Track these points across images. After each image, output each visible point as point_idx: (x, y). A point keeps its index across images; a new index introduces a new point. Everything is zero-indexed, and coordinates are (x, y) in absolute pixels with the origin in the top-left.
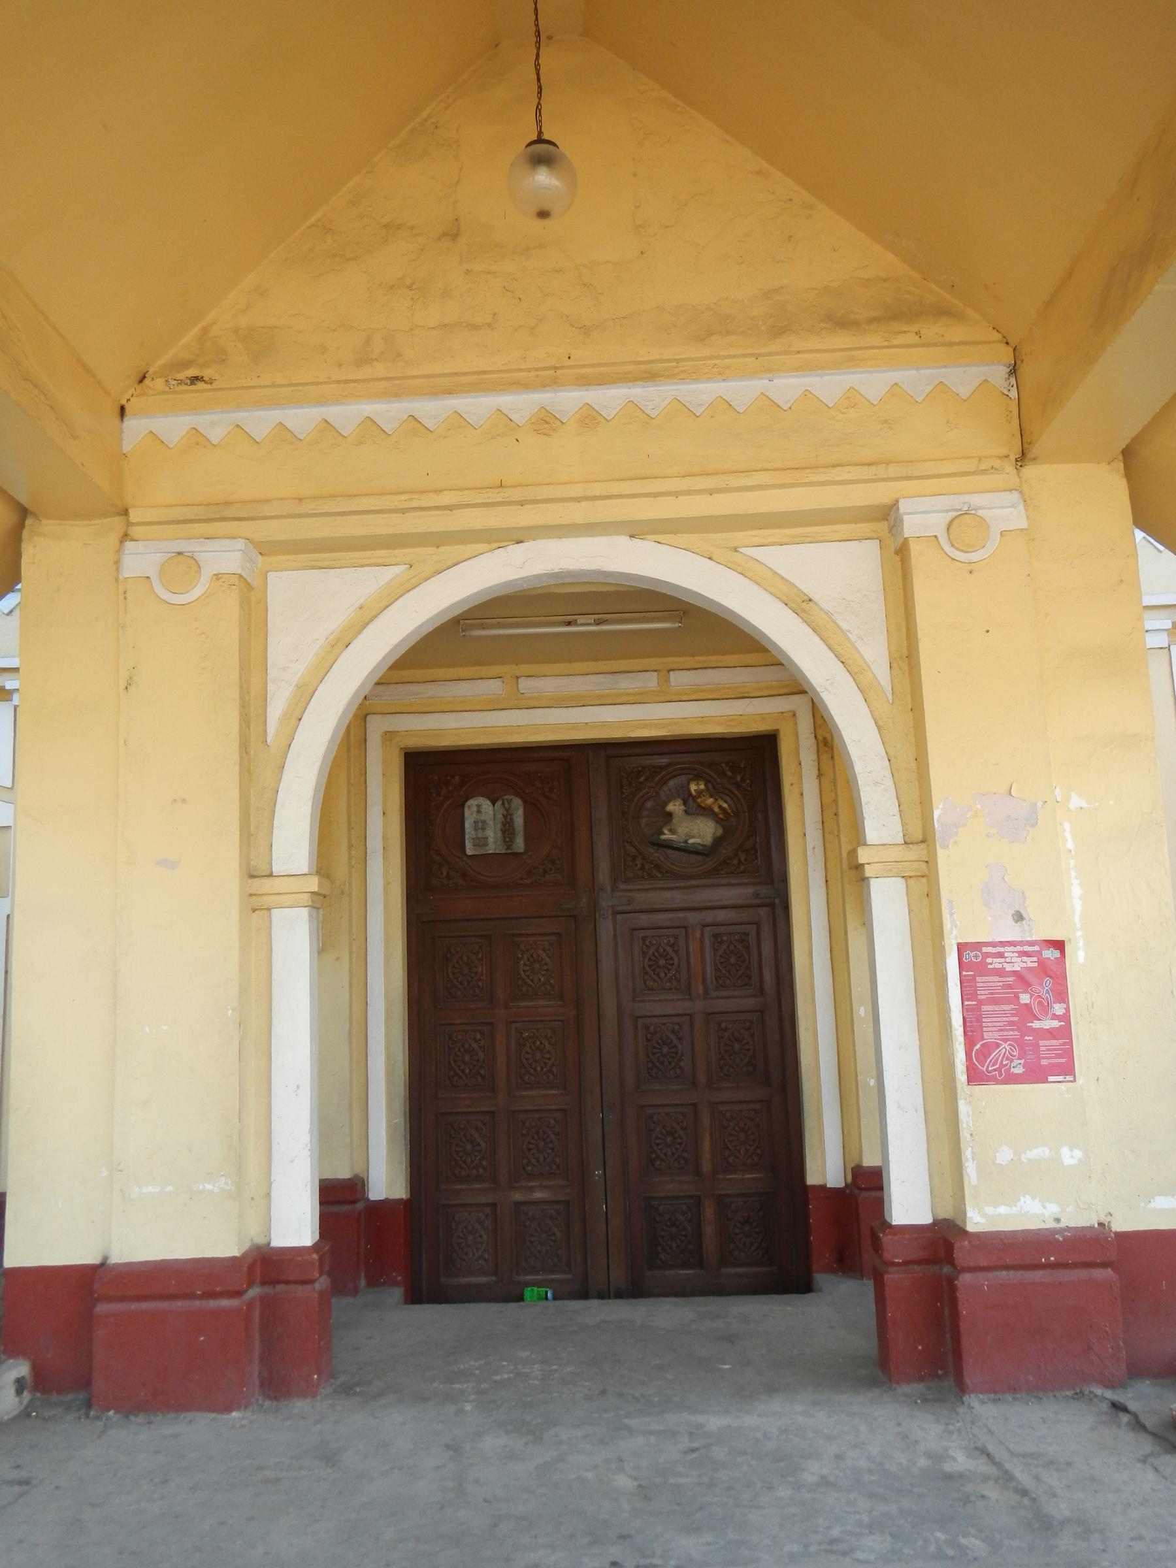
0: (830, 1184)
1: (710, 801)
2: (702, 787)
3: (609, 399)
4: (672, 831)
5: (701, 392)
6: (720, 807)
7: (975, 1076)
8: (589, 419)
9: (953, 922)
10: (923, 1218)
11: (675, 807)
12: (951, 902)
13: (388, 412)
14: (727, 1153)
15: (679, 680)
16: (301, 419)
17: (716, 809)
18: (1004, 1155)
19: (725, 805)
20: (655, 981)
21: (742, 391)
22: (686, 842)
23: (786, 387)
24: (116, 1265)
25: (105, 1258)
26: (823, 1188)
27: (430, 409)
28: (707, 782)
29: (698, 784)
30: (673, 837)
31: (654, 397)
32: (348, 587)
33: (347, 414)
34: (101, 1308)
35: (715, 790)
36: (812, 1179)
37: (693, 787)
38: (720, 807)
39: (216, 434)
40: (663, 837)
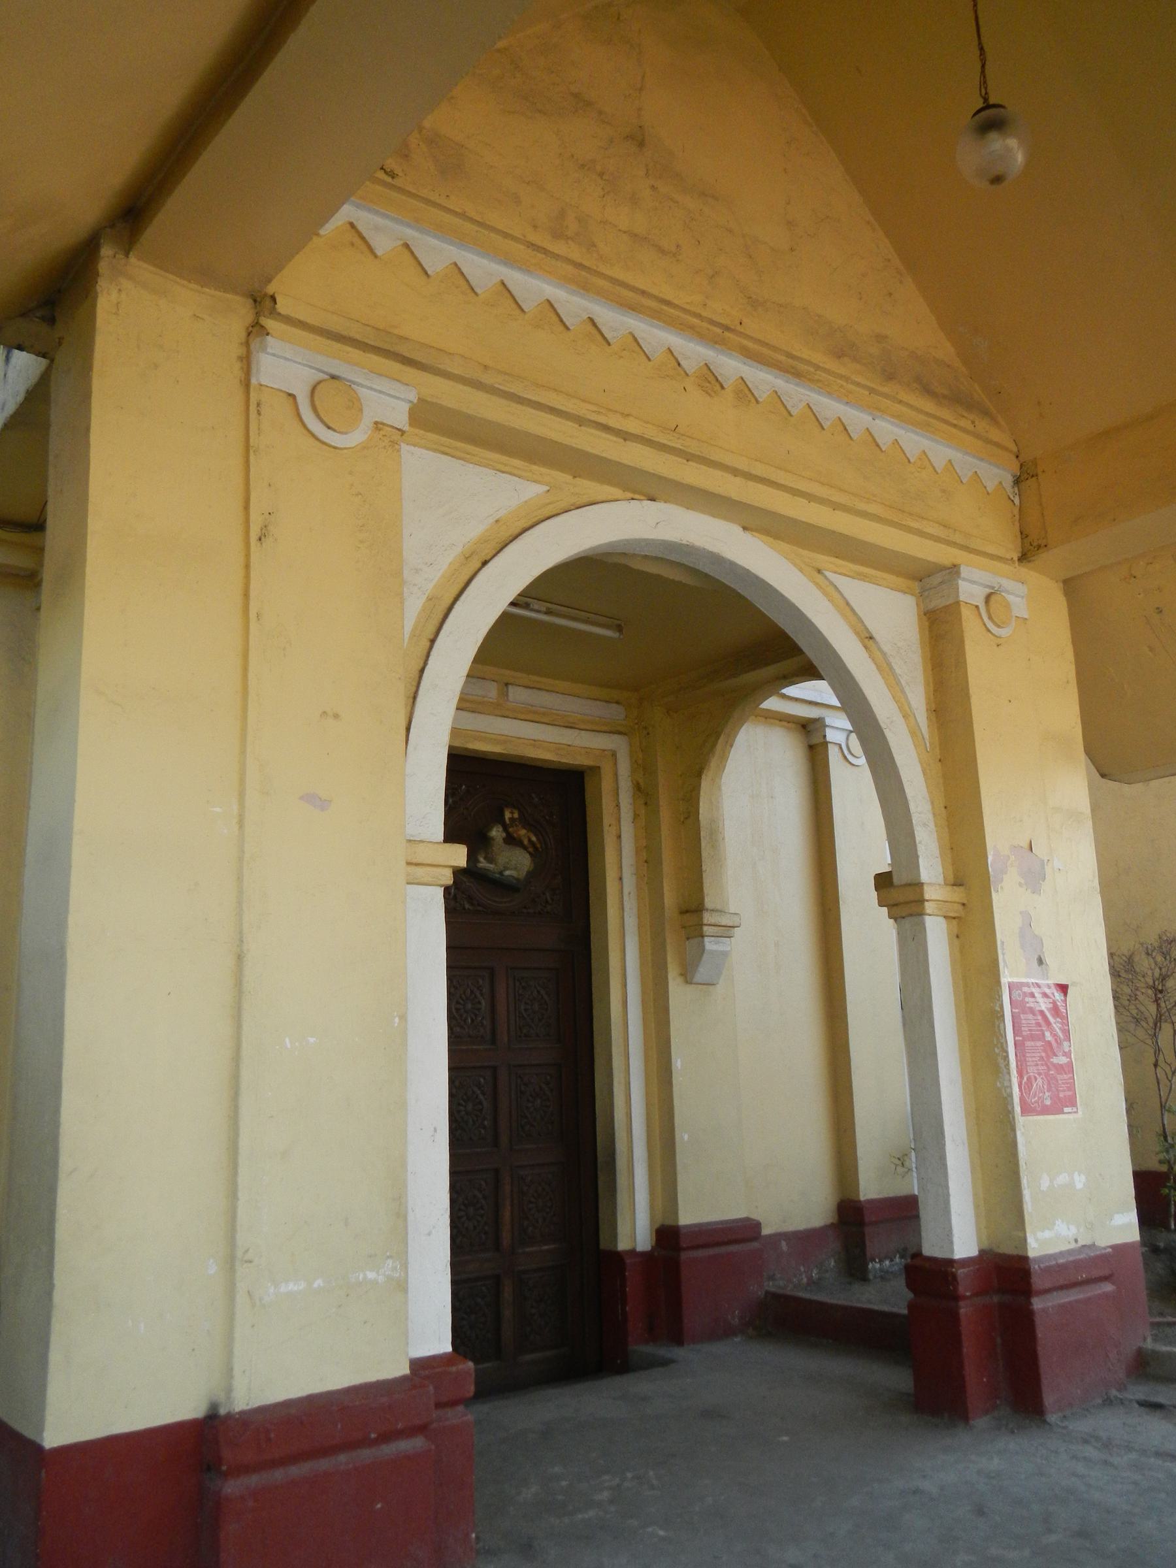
0: (639, 1249)
1: (523, 832)
2: (516, 815)
3: (763, 379)
4: (490, 860)
5: (830, 407)
6: (530, 840)
7: (1026, 1110)
8: (745, 393)
9: (1004, 961)
10: (973, 1252)
11: (496, 833)
12: (1003, 943)
13: (574, 305)
14: (526, 1223)
15: (518, 695)
16: (483, 269)
17: (526, 842)
18: (1045, 1184)
19: (534, 839)
20: (462, 1027)
21: (857, 419)
22: (501, 873)
23: (886, 430)
24: (242, 1413)
25: (213, 1409)
26: (633, 1252)
27: (613, 320)
28: (520, 813)
29: (512, 813)
30: (491, 866)
31: (797, 394)
32: (489, 492)
33: (534, 288)
34: (232, 1487)
35: (525, 821)
36: (623, 1245)
37: (507, 815)
38: (530, 840)
39: (383, 244)
40: (480, 865)
